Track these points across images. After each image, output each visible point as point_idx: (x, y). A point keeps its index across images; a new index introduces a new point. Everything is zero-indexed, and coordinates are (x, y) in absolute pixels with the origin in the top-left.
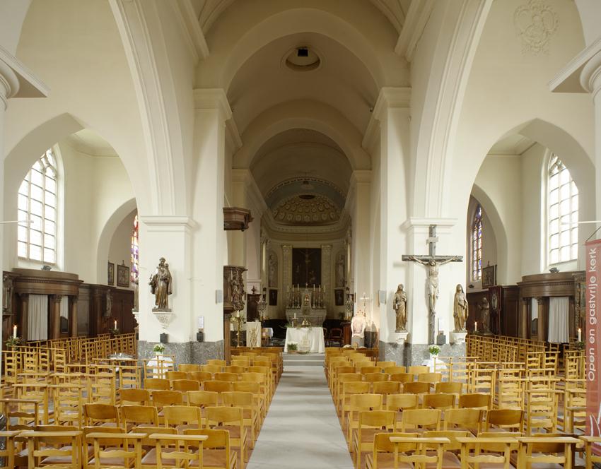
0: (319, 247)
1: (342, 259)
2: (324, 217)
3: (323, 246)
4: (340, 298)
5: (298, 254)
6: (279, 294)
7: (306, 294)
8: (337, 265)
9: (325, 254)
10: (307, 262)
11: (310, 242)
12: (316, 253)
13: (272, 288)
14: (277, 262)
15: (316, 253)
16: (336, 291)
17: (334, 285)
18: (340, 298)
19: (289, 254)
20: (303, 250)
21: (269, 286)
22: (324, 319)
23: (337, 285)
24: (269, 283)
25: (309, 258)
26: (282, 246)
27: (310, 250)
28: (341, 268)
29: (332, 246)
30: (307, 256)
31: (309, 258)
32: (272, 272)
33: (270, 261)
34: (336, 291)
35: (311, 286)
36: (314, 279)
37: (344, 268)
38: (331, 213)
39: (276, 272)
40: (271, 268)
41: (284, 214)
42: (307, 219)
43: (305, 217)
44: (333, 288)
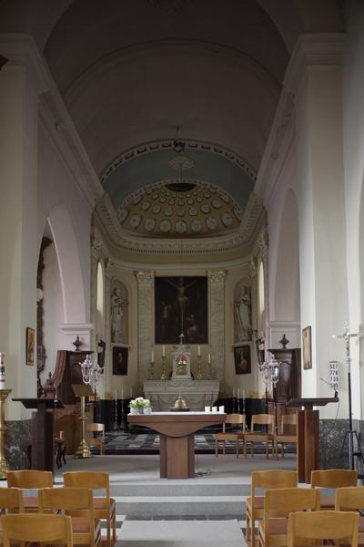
0: (203, 274)
1: (246, 293)
2: (212, 223)
3: (210, 273)
4: (244, 361)
5: (164, 286)
6: (130, 354)
7: (182, 354)
8: (237, 304)
9: (214, 286)
10: (181, 299)
11: (185, 266)
12: (198, 286)
13: (117, 345)
14: (127, 300)
15: (200, 284)
17: (233, 341)
18: (244, 361)
19: (148, 286)
20: (176, 279)
21: (113, 341)
23: (237, 339)
24: (113, 334)
25: (186, 294)
26: (135, 273)
27: (187, 279)
28: (244, 309)
29: (226, 272)
30: (182, 290)
31: (186, 294)
33: (115, 298)
34: (235, 349)
35: (187, 341)
36: (194, 328)
37: (250, 306)
38: (226, 215)
39: (125, 319)
40: (116, 310)
41: (138, 218)
42: (180, 227)
43: (177, 224)
44: (230, 343)
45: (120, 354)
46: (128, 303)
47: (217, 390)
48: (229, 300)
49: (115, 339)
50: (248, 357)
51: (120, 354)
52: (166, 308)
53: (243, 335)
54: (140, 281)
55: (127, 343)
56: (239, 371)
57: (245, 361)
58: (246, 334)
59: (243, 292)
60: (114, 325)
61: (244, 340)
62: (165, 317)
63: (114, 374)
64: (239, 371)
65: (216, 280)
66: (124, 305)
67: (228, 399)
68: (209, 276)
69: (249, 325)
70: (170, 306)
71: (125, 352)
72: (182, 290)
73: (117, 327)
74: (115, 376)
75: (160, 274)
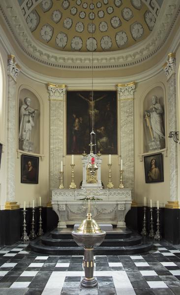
0: (113, 89)
1: (156, 102)
4: (155, 170)
8: (146, 114)
9: (123, 98)
10: (92, 112)
11: (95, 81)
12: (109, 99)
14: (38, 110)
15: (109, 99)
16: (145, 157)
18: (155, 170)
19: (60, 98)
20: (86, 93)
22: (129, 207)
23: (146, 148)
24: (21, 142)
26: (47, 85)
27: (98, 94)
28: (155, 118)
29: (136, 84)
30: (92, 103)
31: (96, 107)
32: (28, 126)
37: (162, 115)
39: (37, 128)
44: (140, 152)
45: (30, 162)
46: (39, 115)
47: (129, 198)
48: (139, 110)
49: (24, 147)
50: (160, 165)
51: (30, 162)
52: (77, 120)
53: (153, 143)
54: (52, 94)
55: (39, 153)
56: (149, 180)
57: (157, 169)
58: (158, 143)
59: (154, 102)
60: (24, 133)
61: (156, 149)
62: (76, 129)
63: (23, 181)
64: (149, 180)
65: (126, 93)
66: (36, 115)
67: (138, 208)
68: (119, 89)
69: (159, 133)
70: (81, 119)
71: (35, 161)
72: (92, 103)
73: (27, 136)
74: (22, 184)
75: (71, 89)
